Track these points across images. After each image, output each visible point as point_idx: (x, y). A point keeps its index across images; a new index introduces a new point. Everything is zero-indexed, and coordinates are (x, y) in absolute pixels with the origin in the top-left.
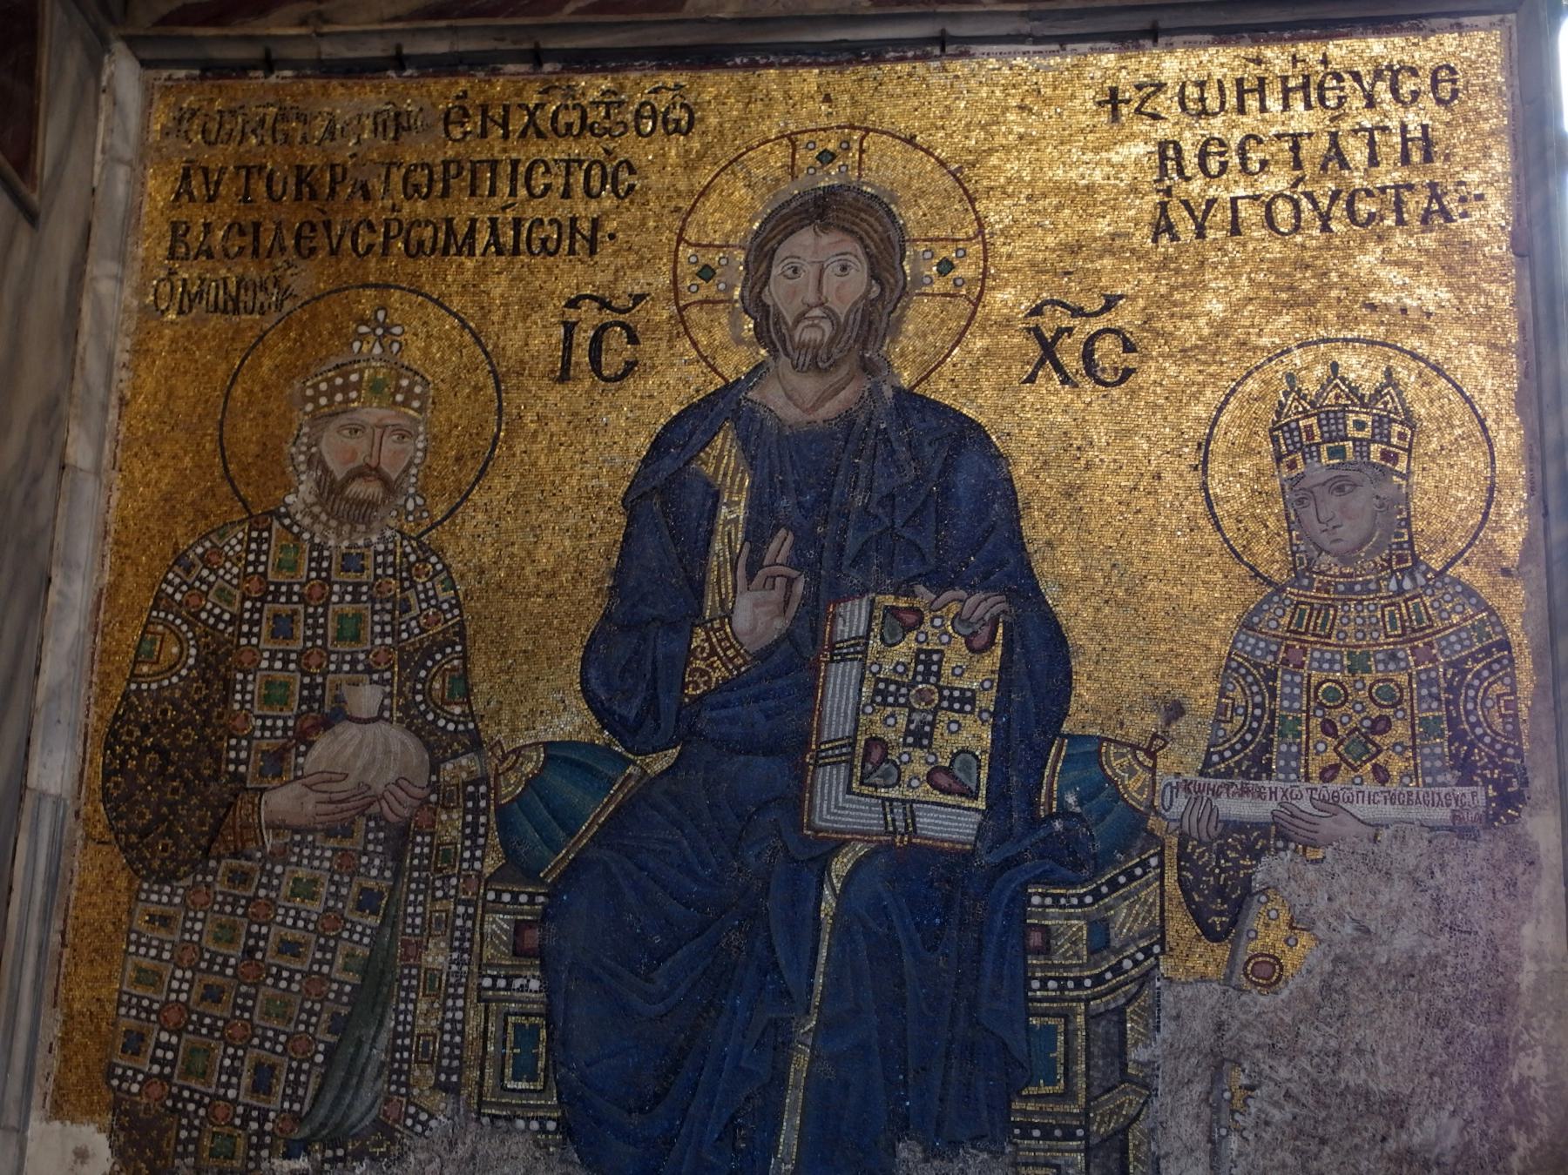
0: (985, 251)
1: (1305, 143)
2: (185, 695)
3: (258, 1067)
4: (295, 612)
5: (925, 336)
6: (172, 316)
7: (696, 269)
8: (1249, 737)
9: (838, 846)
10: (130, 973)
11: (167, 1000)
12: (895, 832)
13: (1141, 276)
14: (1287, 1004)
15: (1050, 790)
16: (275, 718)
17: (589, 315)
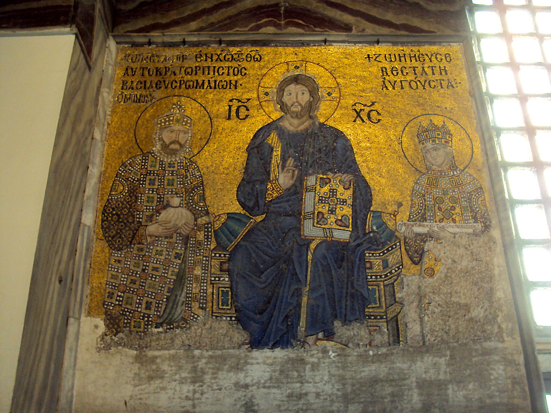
1: (416, 69)
2: (125, 200)
3: (147, 302)
4: (155, 178)
6: (122, 103)
8: (420, 211)
10: (110, 276)
11: (120, 284)
12: (327, 237)
14: (436, 281)
15: (369, 225)
16: (150, 206)
17: (235, 104)
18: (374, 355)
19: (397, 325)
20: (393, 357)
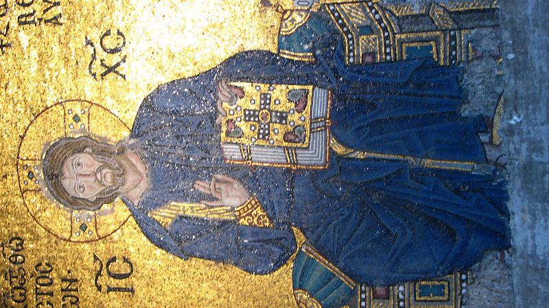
0: (68, 101)
5: (106, 126)
7: (82, 232)
9: (332, 152)
12: (325, 126)
13: (77, 30)
17: (105, 280)
18: (515, 53)
19: (466, 12)
20: (518, 21)
